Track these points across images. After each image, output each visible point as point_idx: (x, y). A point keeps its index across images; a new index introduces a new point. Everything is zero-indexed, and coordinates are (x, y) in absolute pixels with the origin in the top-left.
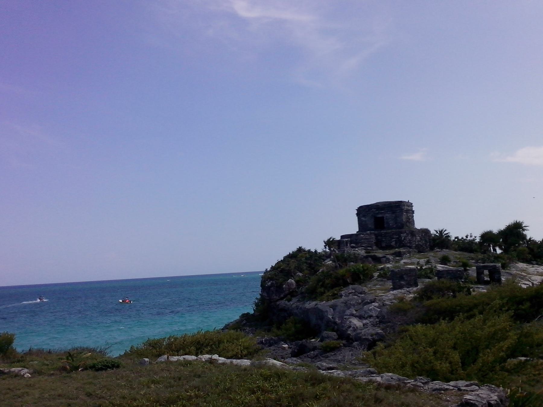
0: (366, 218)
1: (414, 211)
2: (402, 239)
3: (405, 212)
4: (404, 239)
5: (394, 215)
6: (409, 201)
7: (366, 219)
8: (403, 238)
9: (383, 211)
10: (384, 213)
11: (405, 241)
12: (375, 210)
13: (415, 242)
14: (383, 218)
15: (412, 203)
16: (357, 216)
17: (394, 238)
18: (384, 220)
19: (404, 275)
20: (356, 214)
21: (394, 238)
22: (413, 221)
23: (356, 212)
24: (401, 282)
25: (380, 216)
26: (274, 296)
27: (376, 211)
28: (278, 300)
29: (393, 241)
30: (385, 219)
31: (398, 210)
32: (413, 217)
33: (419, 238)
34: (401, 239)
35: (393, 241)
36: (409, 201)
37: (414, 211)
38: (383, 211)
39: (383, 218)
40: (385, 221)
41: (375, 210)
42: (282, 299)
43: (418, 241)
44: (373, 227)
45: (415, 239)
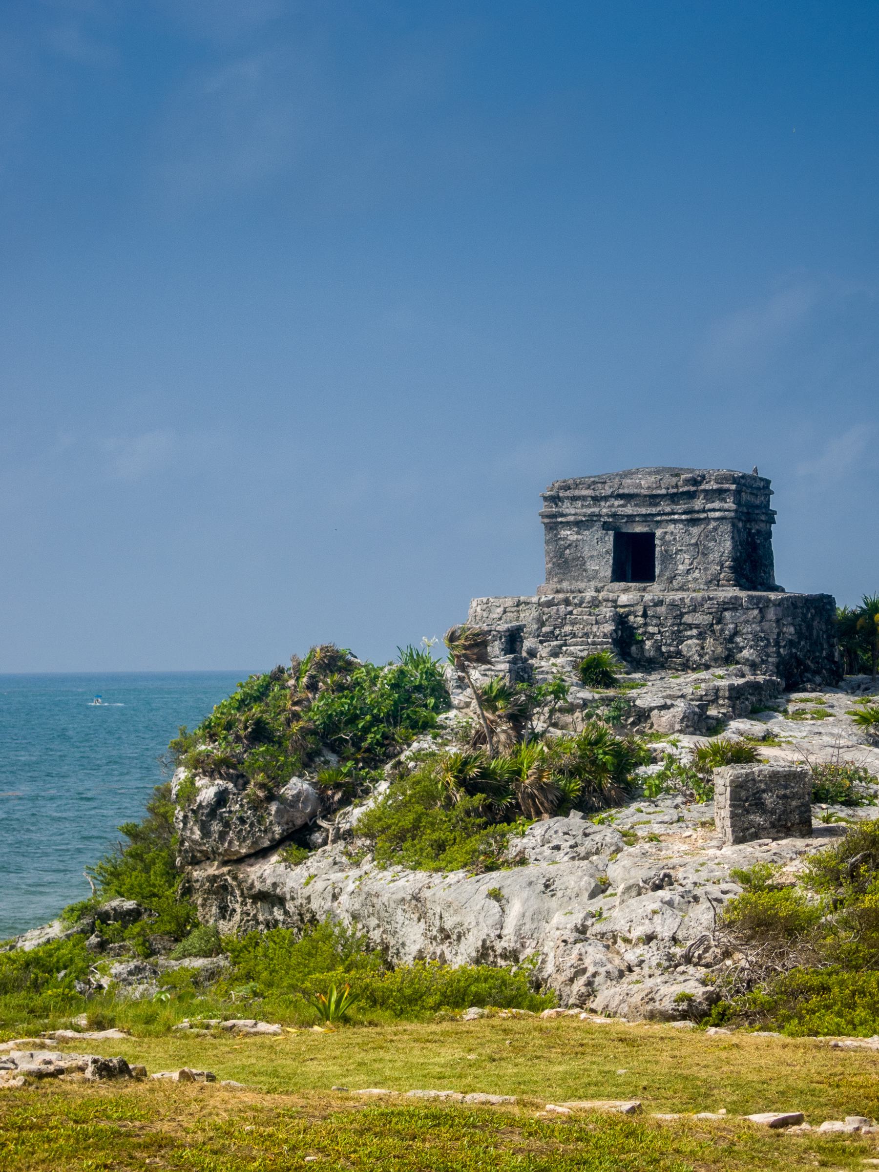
0: (578, 533)
1: (775, 513)
4: (736, 633)
6: (756, 471)
7: (580, 537)
8: (732, 626)
11: (738, 639)
12: (622, 502)
15: (768, 482)
18: (654, 546)
19: (764, 791)
22: (771, 554)
24: (752, 817)
25: (639, 529)
26: (230, 843)
28: (241, 860)
30: (657, 542)
31: (714, 510)
32: (769, 535)
33: (792, 629)
34: (722, 630)
35: (691, 637)
36: (756, 471)
37: (775, 513)
39: (651, 536)
40: (657, 549)
42: (262, 854)
43: (791, 643)
44: (609, 573)
45: (778, 634)
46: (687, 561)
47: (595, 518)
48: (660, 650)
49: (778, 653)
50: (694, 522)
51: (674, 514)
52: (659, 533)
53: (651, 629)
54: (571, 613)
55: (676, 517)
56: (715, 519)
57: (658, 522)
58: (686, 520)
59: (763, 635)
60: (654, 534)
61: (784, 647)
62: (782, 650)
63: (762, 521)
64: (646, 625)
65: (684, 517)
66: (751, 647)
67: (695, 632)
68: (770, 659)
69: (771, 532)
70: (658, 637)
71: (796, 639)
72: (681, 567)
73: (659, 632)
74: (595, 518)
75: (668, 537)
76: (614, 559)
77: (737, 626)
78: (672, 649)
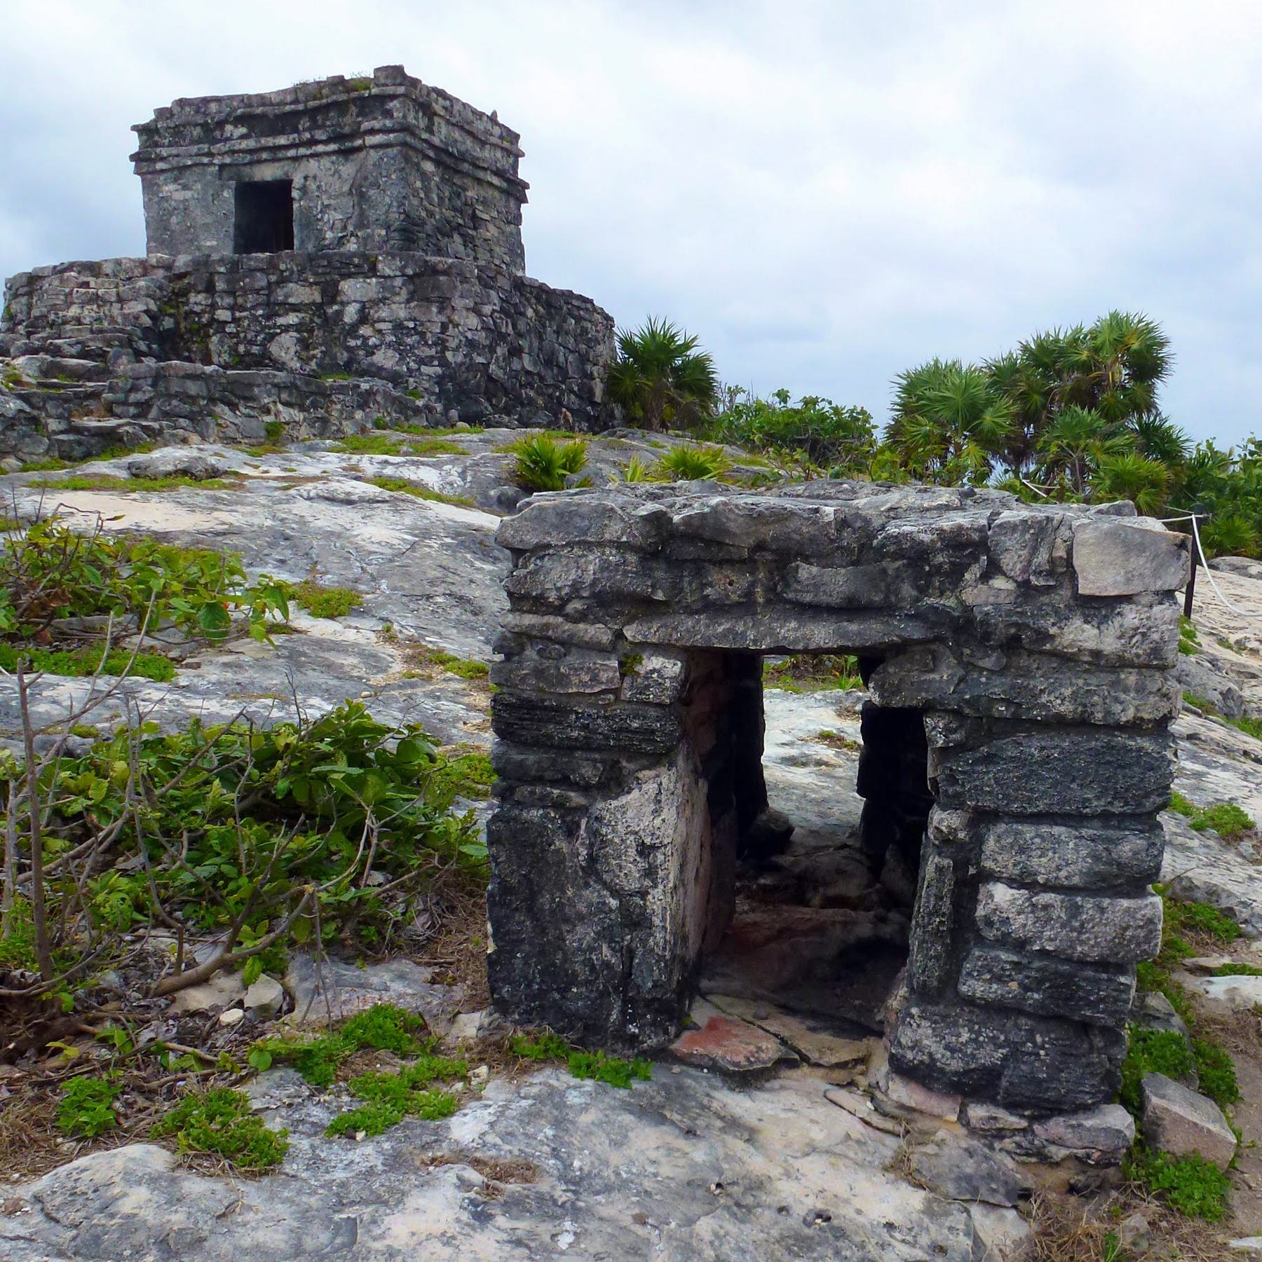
0: (185, 187)
1: (526, 186)
2: (347, 319)
3: (431, 154)
4: (364, 319)
5: (348, 169)
6: (494, 113)
7: (188, 194)
9: (282, 140)
10: (292, 153)
11: (365, 330)
12: (243, 130)
13: (441, 344)
14: (284, 186)
16: (138, 171)
17: (295, 308)
18: (291, 200)
20: (133, 158)
21: (295, 308)
23: (133, 143)
25: (268, 173)
27: (243, 137)
29: (286, 328)
30: (295, 194)
31: (372, 132)
32: (517, 219)
35: (286, 328)
37: (526, 186)
38: (282, 140)
39: (284, 186)
40: (296, 206)
41: (243, 130)
45: (444, 327)
46: (339, 225)
47: (206, 160)
48: (236, 351)
49: (444, 363)
50: (346, 153)
51: (317, 142)
52: (298, 181)
53: (223, 315)
54: (86, 285)
55: (320, 148)
56: (373, 147)
57: (296, 159)
58: (334, 153)
59: (411, 325)
60: (291, 182)
61: (456, 349)
62: (449, 355)
63: (491, 184)
64: (214, 307)
65: (332, 147)
66: (389, 345)
67: (292, 319)
68: (424, 369)
69: (520, 215)
70: (231, 329)
71: (482, 337)
72: (329, 235)
73: (235, 320)
74: (206, 160)
75: (312, 186)
76: (237, 227)
77: (363, 307)
78: (255, 349)
